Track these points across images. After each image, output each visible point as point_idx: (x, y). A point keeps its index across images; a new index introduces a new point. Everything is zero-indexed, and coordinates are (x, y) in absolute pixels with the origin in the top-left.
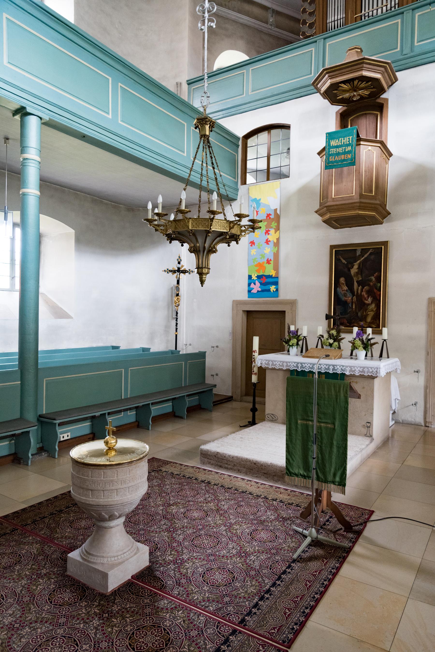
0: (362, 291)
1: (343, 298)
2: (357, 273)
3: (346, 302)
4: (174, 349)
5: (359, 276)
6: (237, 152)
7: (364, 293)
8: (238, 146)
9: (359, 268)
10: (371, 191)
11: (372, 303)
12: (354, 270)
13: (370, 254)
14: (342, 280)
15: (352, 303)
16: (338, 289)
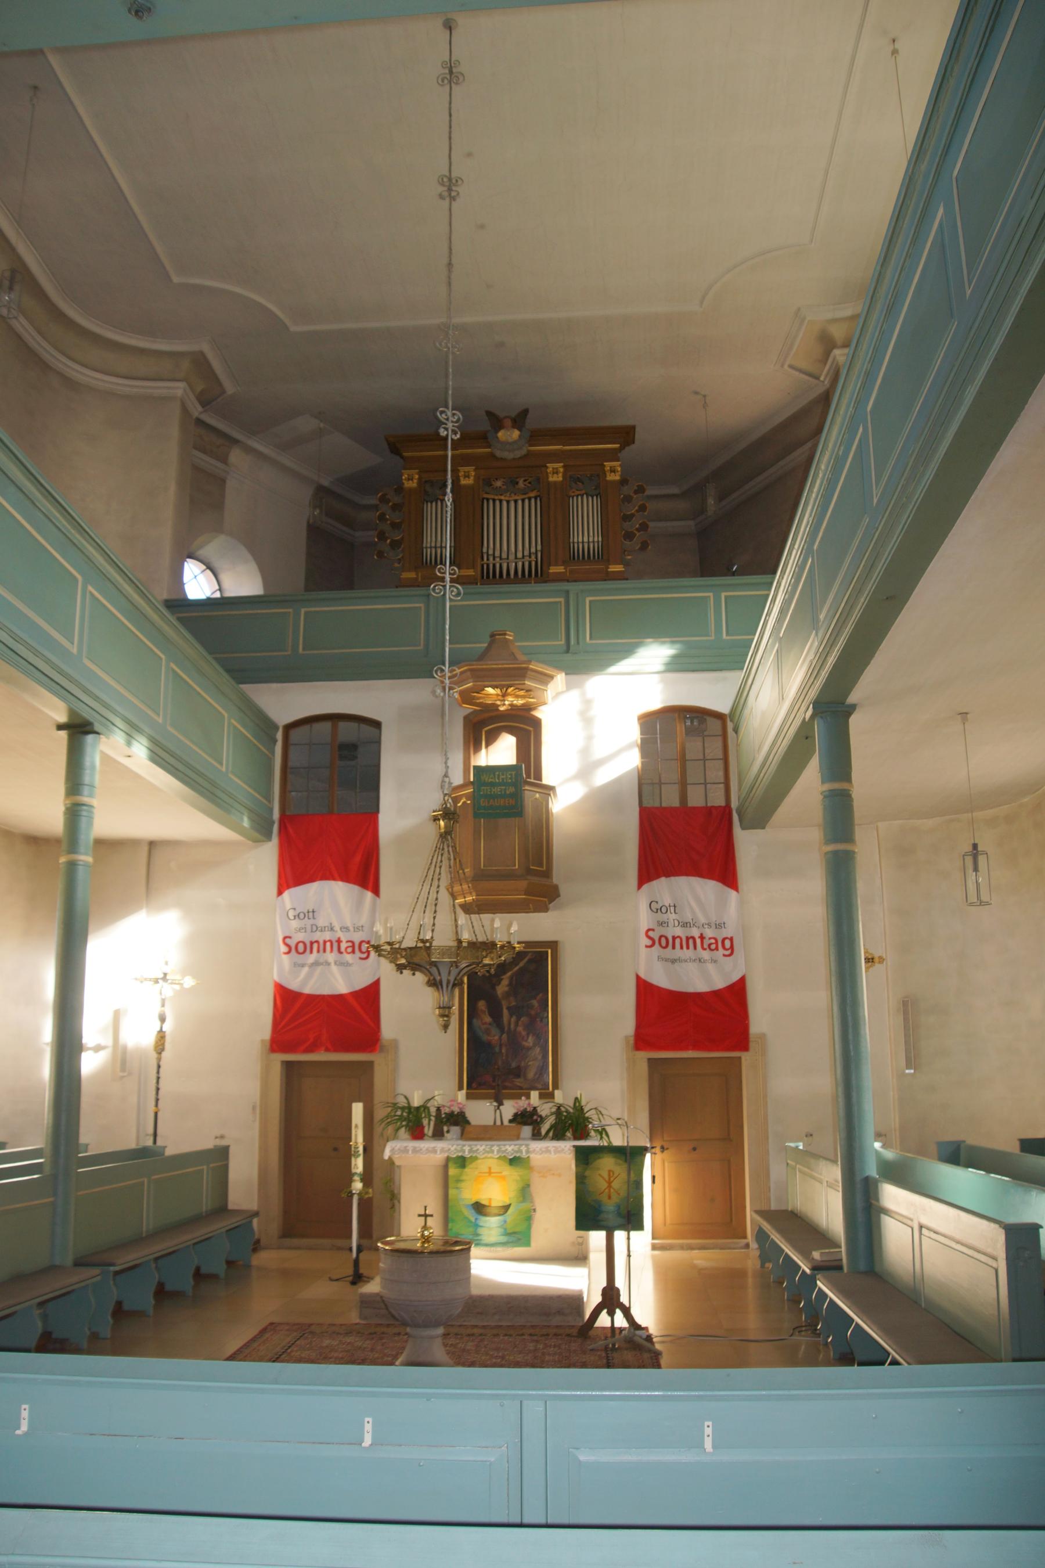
0: (517, 1024)
1: (485, 1038)
2: (507, 995)
3: (489, 1045)
4: (149, 1142)
5: (512, 998)
6: (273, 753)
7: (520, 1029)
8: (275, 741)
9: (510, 984)
10: (541, 865)
11: (535, 1045)
12: (502, 988)
13: (530, 961)
14: (482, 1005)
15: (501, 1046)
16: (475, 1021)
